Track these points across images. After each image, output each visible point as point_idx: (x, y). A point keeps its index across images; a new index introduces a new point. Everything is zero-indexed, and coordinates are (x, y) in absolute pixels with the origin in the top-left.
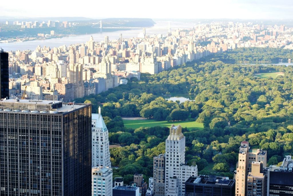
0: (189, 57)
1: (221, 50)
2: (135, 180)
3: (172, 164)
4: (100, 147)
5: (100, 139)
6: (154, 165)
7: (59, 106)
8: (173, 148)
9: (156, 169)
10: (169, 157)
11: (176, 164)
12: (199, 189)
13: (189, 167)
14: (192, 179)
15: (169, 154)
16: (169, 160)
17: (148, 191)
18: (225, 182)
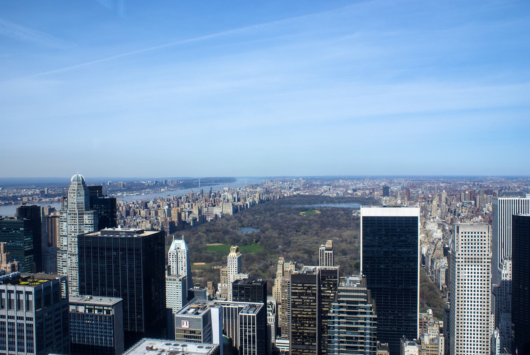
0: (257, 202)
1: (280, 198)
2: (208, 285)
3: (232, 273)
4: (183, 263)
5: (183, 257)
6: (221, 274)
7: (142, 232)
8: (232, 262)
9: (222, 277)
10: (230, 268)
11: (235, 273)
12: (242, 287)
13: (244, 275)
14: (237, 281)
15: (230, 266)
16: (230, 270)
17: (217, 293)
18: (259, 282)
